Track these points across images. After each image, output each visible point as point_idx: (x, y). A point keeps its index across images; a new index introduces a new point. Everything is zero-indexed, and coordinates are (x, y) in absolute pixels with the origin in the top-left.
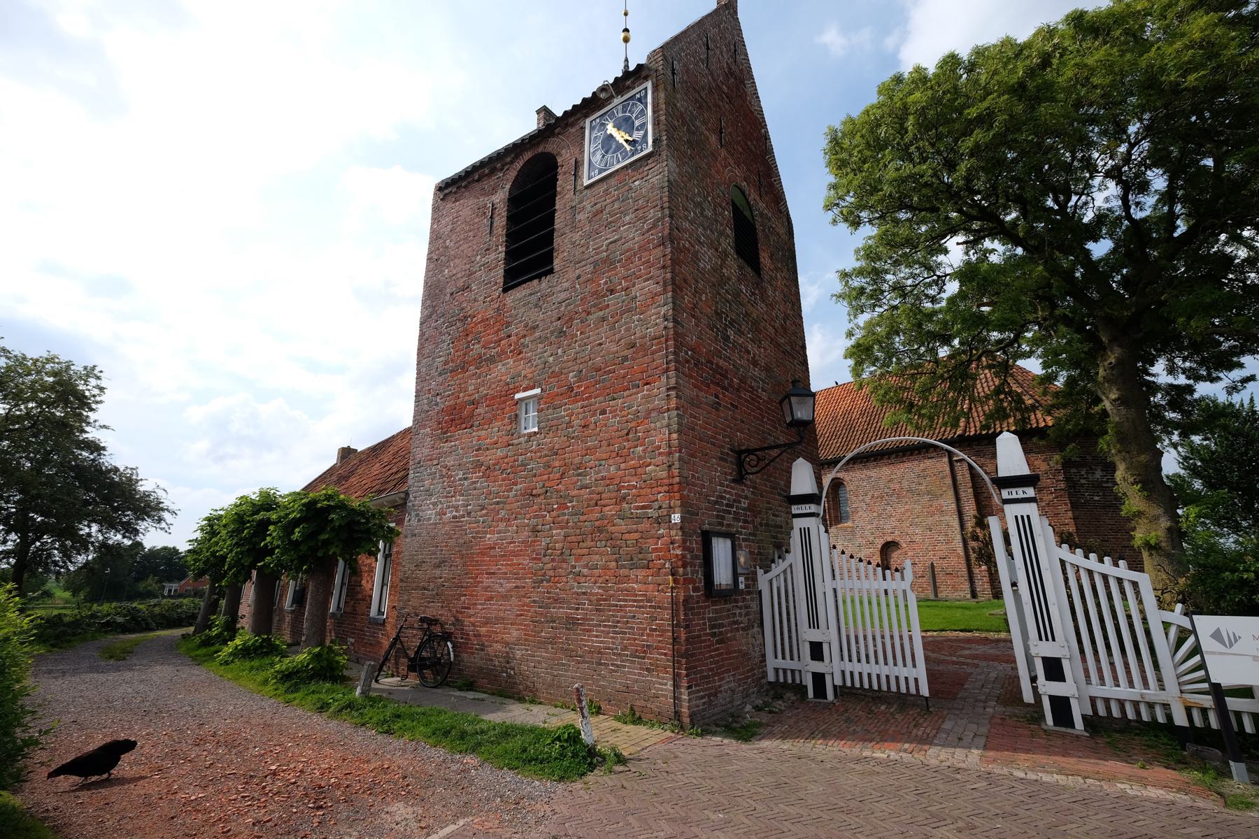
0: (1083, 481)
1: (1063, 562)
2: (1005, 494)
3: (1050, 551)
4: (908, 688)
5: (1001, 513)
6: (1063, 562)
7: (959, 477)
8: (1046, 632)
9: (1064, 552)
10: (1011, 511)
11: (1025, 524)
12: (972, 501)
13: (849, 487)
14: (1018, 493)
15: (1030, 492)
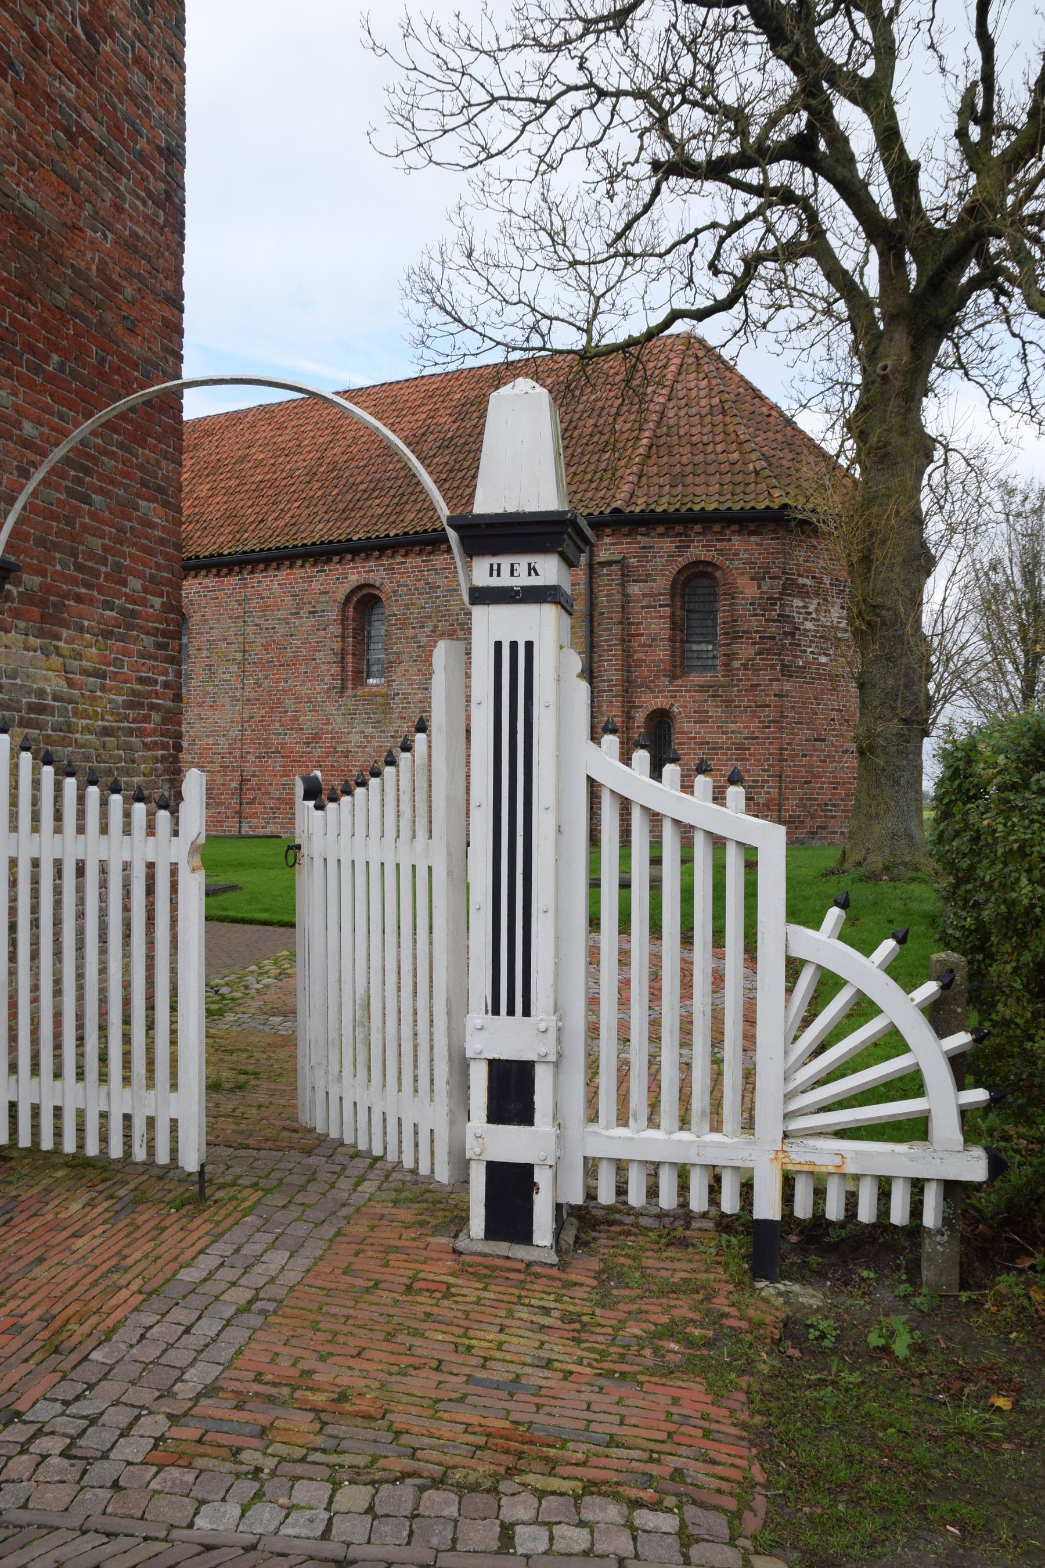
0: (809, 625)
1: (593, 787)
2: (481, 573)
3: (573, 754)
4: (151, 1149)
5: (460, 631)
6: (593, 787)
7: (602, 599)
8: (511, 994)
9: (603, 761)
10: (492, 624)
11: (516, 663)
12: (617, 650)
13: (392, 607)
14: (516, 570)
15: (549, 570)
